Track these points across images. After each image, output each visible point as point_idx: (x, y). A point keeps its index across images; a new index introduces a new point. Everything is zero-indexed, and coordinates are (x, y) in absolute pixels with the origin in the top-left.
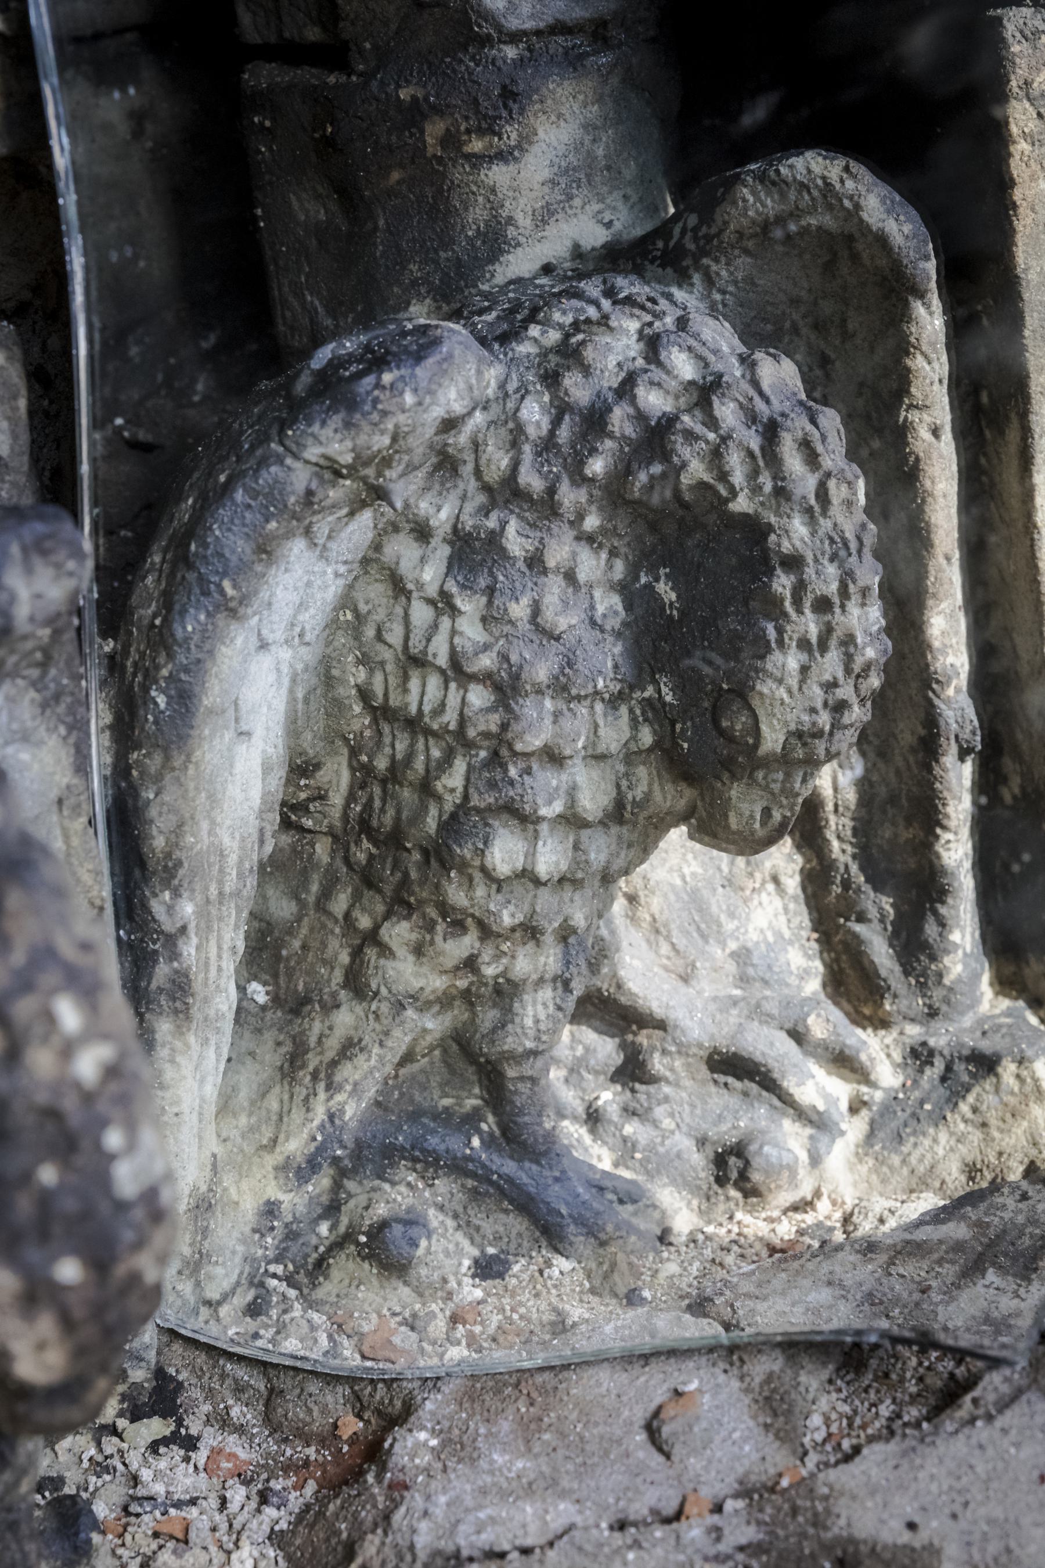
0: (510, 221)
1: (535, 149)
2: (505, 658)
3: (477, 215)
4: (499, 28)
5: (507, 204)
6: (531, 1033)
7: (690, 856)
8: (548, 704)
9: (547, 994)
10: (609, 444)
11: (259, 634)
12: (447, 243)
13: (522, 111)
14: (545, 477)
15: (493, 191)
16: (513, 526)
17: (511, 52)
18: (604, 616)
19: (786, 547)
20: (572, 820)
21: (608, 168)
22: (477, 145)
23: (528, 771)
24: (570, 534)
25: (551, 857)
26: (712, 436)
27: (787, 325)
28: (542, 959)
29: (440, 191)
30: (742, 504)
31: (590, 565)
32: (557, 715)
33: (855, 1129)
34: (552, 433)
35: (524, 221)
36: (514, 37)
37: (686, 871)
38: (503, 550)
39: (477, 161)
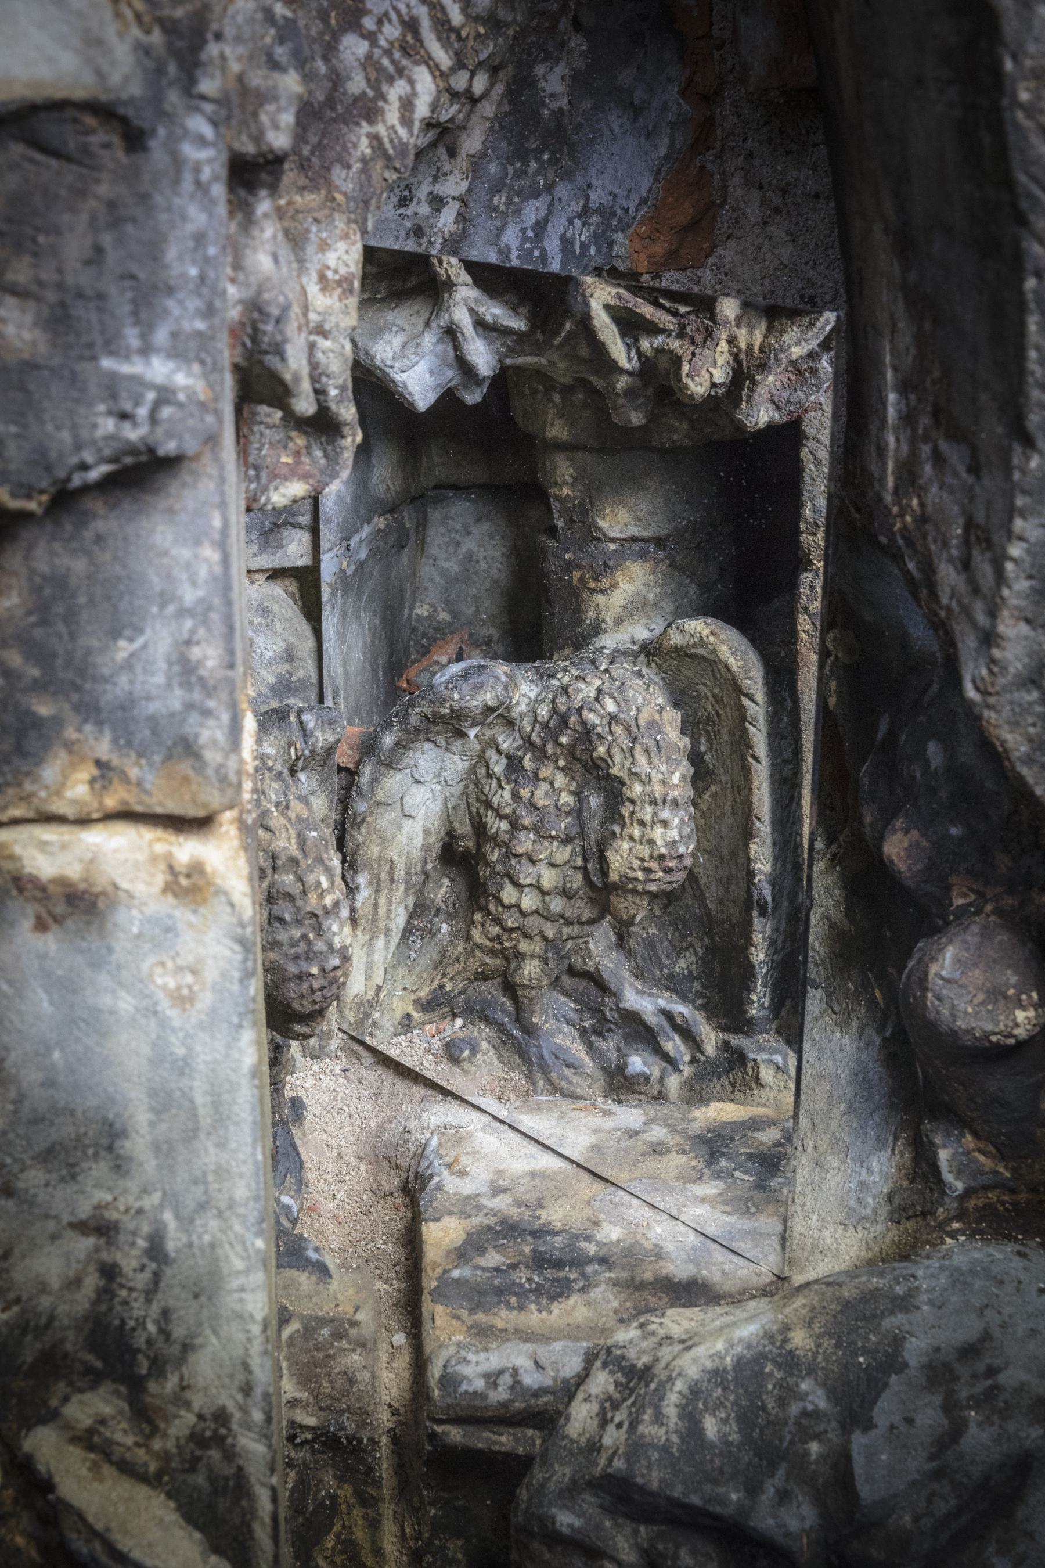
3: (591, 615)
9: (536, 962)
12: (578, 622)
16: (528, 756)
17: (612, 547)
19: (629, 794)
20: (538, 887)
22: (592, 585)
24: (551, 766)
25: (529, 901)
30: (615, 771)
31: (560, 780)
33: (687, 1071)
35: (610, 622)
36: (613, 540)
39: (592, 591)
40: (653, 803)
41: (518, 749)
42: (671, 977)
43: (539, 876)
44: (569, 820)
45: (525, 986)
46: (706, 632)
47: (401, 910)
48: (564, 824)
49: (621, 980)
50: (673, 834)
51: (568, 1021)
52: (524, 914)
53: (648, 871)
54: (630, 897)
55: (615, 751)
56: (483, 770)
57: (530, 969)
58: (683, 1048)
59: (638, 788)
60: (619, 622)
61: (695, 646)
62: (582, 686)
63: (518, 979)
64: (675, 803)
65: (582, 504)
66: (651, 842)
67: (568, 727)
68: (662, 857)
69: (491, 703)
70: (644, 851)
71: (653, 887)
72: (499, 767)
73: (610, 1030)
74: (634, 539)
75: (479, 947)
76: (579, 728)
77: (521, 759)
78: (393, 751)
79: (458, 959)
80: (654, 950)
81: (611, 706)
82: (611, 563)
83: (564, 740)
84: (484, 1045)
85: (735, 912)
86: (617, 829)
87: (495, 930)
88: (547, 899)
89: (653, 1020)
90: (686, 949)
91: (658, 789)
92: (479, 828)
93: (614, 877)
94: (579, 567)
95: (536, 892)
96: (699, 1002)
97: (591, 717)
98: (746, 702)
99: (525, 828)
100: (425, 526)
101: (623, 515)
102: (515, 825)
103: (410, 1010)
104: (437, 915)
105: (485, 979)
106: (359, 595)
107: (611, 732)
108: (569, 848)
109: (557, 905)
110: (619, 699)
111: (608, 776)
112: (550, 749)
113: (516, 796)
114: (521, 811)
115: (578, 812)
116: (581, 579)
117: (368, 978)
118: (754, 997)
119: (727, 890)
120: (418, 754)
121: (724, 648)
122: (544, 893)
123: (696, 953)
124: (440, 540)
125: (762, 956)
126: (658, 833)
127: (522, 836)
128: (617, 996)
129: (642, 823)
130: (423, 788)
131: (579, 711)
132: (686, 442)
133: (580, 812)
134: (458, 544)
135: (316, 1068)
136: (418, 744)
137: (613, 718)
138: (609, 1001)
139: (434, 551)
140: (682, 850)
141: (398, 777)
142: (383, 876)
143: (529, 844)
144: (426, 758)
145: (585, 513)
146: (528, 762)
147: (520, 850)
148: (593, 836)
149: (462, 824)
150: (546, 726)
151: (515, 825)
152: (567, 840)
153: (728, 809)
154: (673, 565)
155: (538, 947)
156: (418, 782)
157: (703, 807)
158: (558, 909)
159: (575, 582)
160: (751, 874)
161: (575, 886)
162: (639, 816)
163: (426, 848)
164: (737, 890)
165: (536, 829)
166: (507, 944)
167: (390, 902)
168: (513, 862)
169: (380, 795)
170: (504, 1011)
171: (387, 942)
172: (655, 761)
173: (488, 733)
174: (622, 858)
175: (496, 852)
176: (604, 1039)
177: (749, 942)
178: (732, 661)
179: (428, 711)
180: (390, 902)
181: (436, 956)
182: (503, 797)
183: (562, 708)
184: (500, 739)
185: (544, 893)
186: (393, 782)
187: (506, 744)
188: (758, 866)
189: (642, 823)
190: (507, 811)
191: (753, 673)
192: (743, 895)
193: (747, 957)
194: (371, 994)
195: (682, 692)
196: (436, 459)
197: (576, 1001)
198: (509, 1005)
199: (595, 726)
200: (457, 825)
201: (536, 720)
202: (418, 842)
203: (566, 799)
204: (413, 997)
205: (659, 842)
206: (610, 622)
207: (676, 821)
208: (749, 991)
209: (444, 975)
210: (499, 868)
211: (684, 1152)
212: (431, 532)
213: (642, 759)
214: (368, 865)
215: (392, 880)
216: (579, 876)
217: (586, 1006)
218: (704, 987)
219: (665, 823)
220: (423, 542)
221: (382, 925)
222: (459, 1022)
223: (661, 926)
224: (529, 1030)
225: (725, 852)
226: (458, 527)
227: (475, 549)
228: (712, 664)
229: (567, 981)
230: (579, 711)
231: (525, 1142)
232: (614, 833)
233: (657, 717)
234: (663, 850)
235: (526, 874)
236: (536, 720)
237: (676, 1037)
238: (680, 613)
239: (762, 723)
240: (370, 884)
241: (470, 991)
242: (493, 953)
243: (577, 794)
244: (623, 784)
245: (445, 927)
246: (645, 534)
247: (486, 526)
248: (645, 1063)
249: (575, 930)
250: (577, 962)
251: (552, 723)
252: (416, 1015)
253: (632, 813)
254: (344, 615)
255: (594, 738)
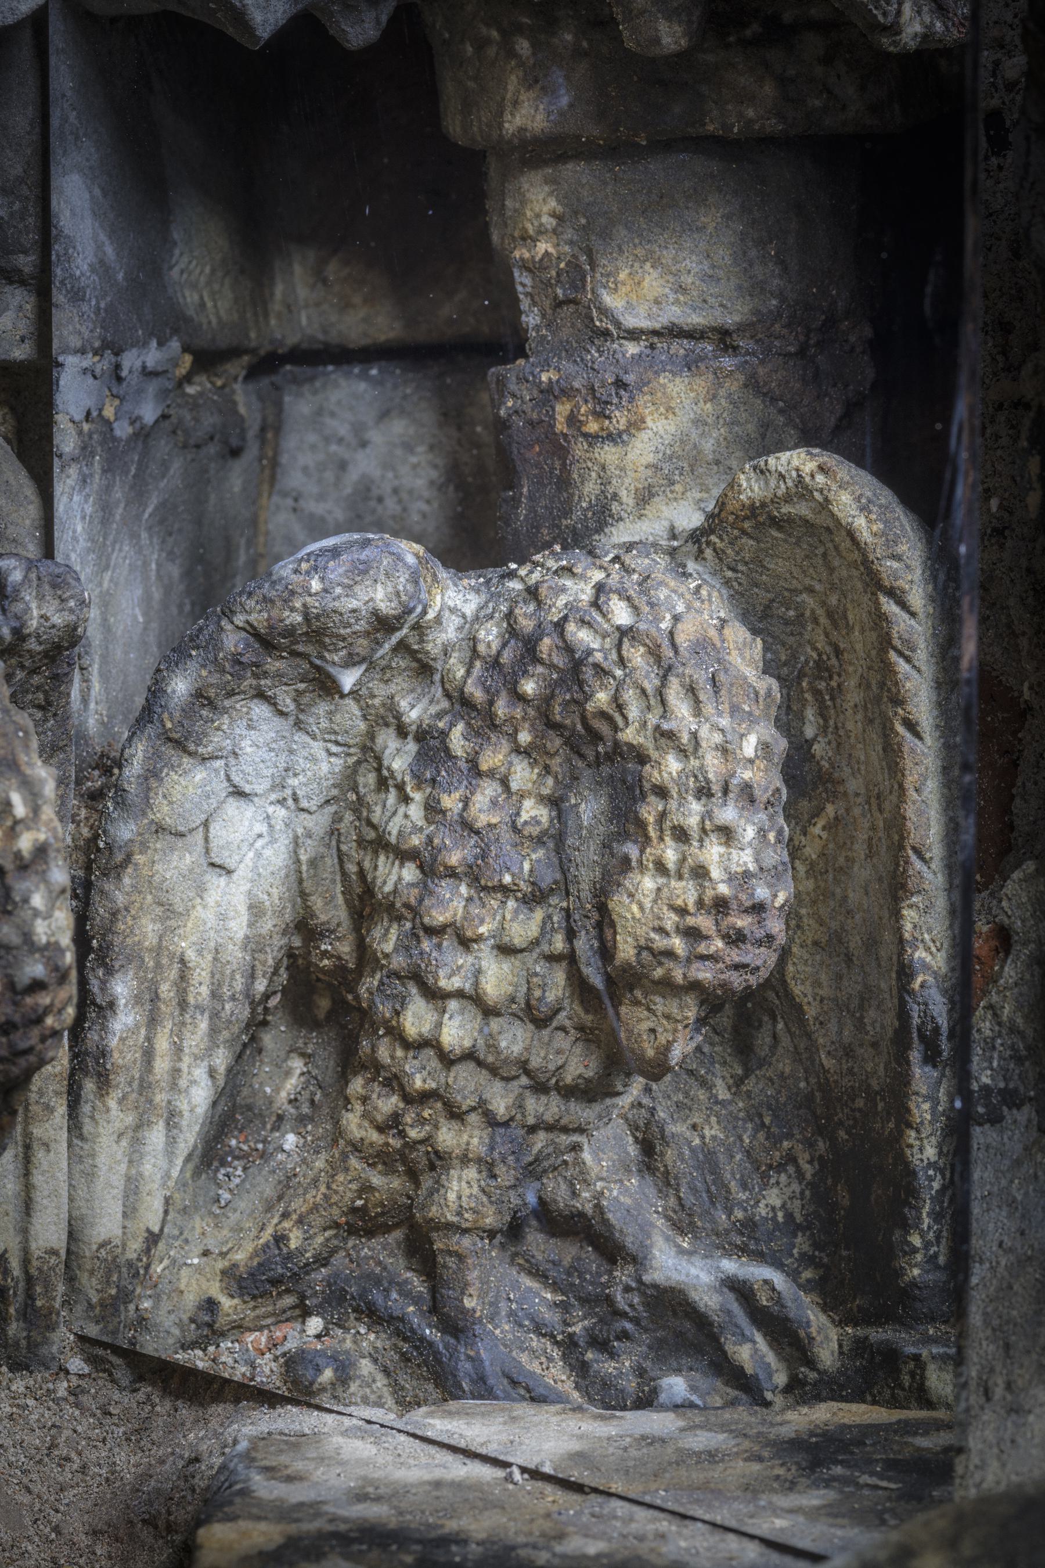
0: (615, 496)
1: (644, 435)
2: (430, 840)
3: (591, 488)
4: (618, 324)
5: (614, 482)
6: (454, 1207)
7: (713, 1119)
8: (463, 889)
9: (471, 1173)
10: (540, 669)
11: (229, 779)
13: (632, 399)
14: (487, 690)
15: (604, 468)
16: (460, 727)
17: (632, 349)
18: (526, 823)
19: (656, 777)
20: (474, 999)
21: (717, 463)
22: (593, 427)
23: (439, 946)
24: (505, 746)
25: (456, 1031)
26: (619, 673)
27: (808, 613)
28: (465, 1137)
29: (564, 464)
30: (629, 735)
31: (522, 775)
32: (469, 899)
34: (499, 653)
35: (628, 499)
36: (634, 335)
37: (707, 1133)
38: (447, 750)
39: (592, 439)
40: (704, 792)
41: (439, 716)
42: (749, 1225)
43: (478, 972)
44: (539, 854)
45: (449, 1226)
46: (810, 466)
47: (200, 1073)
48: (527, 864)
49: (646, 1229)
50: (745, 859)
51: (539, 1329)
52: (447, 1060)
53: (693, 934)
54: (660, 1004)
55: (629, 695)
56: (371, 778)
57: (460, 1190)
58: (771, 1358)
59: (673, 764)
60: (645, 497)
61: (788, 499)
62: (568, 583)
63: (434, 1212)
64: (747, 788)
65: (574, 266)
66: (700, 873)
67: (537, 660)
68: (721, 905)
69: (386, 607)
70: (687, 892)
71: (704, 973)
72: (399, 758)
73: (624, 1336)
74: (674, 332)
75: (356, 1147)
76: (559, 660)
77: (444, 734)
78: (188, 712)
79: (315, 1181)
80: (715, 1169)
81: (621, 614)
82: (630, 378)
83: (529, 687)
84: (366, 1366)
85: (875, 1067)
86: (632, 850)
87: (388, 1104)
88: (495, 1024)
89: (709, 1300)
90: (780, 1168)
91: (713, 764)
92: (366, 905)
93: (626, 950)
94: (568, 393)
95: (472, 1009)
96: (807, 1274)
97: (583, 637)
98: (889, 607)
99: (452, 873)
100: (278, 429)
101: (653, 283)
102: (431, 868)
103: (215, 1290)
104: (275, 1128)
105: (370, 1234)
106: (138, 492)
107: (622, 662)
108: (539, 914)
109: (513, 1039)
110: (641, 602)
111: (619, 751)
112: (502, 708)
113: (433, 809)
114: (444, 838)
115: (556, 840)
116: (572, 420)
117: (129, 1212)
118: (916, 1241)
119: (860, 1025)
120: (240, 729)
121: (845, 498)
122: (489, 1012)
123: (800, 1175)
124: (307, 459)
125: (930, 1152)
126: (713, 854)
127: (444, 888)
128: (637, 1261)
129: (681, 835)
130: (248, 811)
131: (560, 626)
132: (773, 126)
133: (560, 839)
134: (343, 466)
135: (19, 1386)
136: (239, 704)
137: (623, 632)
138: (623, 1275)
139: (294, 479)
140: (762, 893)
141: (200, 775)
142: (166, 990)
143: (457, 907)
144: (254, 738)
145: (576, 276)
146: (458, 741)
147: (439, 917)
148: (586, 877)
149: (329, 901)
150: (494, 663)
151: (431, 868)
152: (535, 898)
153: (860, 849)
154: (752, 384)
155: (473, 1138)
156: (238, 793)
157: (811, 851)
158: (516, 1049)
159: (561, 426)
160: (905, 972)
161: (551, 996)
162: (676, 818)
163: (254, 945)
164: (881, 1021)
165: (473, 875)
166: (413, 1134)
167: (178, 1050)
168: (426, 945)
169: (162, 811)
170: (406, 1294)
171: (171, 1142)
172: (709, 709)
173: (381, 691)
174: (644, 904)
175: (394, 932)
176: (613, 1355)
177: (903, 1119)
178: (860, 522)
179: (258, 618)
180: (178, 1050)
181: (269, 1190)
182: (406, 819)
183: (526, 625)
184: (404, 704)
185: (489, 1012)
186: (190, 785)
187: (415, 712)
188: (920, 954)
189: (681, 835)
190: (416, 841)
191: (902, 548)
192: (891, 1021)
193: (901, 1159)
194: (135, 1246)
195: (766, 613)
196: (302, 292)
197: (555, 1287)
198: (418, 1284)
199: (589, 652)
200: (317, 902)
201: (475, 653)
202: (239, 927)
203: (532, 811)
204: (220, 1265)
205: (715, 873)
206: (628, 499)
207: (750, 833)
208: (906, 1226)
209: (285, 1215)
210: (399, 962)
211: (760, 1459)
212: (290, 442)
213: (681, 708)
214: (135, 957)
215: (183, 1005)
216: (559, 976)
217: (574, 1293)
218: (816, 1245)
219: (727, 833)
220: (275, 464)
221: (160, 1098)
222: (315, 1324)
223: (730, 1123)
224: (457, 1326)
225: (855, 942)
226: (343, 430)
227: (376, 473)
228: (823, 534)
229: (537, 1243)
230: (560, 626)
231: (432, 1450)
232: (626, 860)
233: (713, 633)
234: (723, 889)
235: (452, 970)
236: (475, 653)
237: (759, 1338)
238: (764, 443)
239: (922, 655)
240: (137, 1000)
241: (339, 1260)
242: (383, 1159)
243: (555, 802)
244: (643, 759)
245: (290, 1140)
246: (696, 320)
247: (398, 427)
248: (693, 1389)
249: (550, 1107)
250: (557, 1190)
251: (506, 658)
252: (226, 1303)
253: (662, 816)
254: (105, 509)
255: (588, 673)
